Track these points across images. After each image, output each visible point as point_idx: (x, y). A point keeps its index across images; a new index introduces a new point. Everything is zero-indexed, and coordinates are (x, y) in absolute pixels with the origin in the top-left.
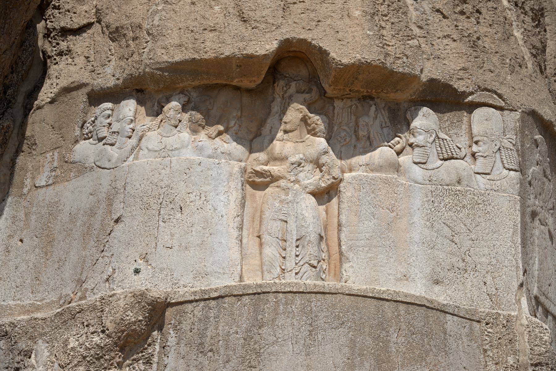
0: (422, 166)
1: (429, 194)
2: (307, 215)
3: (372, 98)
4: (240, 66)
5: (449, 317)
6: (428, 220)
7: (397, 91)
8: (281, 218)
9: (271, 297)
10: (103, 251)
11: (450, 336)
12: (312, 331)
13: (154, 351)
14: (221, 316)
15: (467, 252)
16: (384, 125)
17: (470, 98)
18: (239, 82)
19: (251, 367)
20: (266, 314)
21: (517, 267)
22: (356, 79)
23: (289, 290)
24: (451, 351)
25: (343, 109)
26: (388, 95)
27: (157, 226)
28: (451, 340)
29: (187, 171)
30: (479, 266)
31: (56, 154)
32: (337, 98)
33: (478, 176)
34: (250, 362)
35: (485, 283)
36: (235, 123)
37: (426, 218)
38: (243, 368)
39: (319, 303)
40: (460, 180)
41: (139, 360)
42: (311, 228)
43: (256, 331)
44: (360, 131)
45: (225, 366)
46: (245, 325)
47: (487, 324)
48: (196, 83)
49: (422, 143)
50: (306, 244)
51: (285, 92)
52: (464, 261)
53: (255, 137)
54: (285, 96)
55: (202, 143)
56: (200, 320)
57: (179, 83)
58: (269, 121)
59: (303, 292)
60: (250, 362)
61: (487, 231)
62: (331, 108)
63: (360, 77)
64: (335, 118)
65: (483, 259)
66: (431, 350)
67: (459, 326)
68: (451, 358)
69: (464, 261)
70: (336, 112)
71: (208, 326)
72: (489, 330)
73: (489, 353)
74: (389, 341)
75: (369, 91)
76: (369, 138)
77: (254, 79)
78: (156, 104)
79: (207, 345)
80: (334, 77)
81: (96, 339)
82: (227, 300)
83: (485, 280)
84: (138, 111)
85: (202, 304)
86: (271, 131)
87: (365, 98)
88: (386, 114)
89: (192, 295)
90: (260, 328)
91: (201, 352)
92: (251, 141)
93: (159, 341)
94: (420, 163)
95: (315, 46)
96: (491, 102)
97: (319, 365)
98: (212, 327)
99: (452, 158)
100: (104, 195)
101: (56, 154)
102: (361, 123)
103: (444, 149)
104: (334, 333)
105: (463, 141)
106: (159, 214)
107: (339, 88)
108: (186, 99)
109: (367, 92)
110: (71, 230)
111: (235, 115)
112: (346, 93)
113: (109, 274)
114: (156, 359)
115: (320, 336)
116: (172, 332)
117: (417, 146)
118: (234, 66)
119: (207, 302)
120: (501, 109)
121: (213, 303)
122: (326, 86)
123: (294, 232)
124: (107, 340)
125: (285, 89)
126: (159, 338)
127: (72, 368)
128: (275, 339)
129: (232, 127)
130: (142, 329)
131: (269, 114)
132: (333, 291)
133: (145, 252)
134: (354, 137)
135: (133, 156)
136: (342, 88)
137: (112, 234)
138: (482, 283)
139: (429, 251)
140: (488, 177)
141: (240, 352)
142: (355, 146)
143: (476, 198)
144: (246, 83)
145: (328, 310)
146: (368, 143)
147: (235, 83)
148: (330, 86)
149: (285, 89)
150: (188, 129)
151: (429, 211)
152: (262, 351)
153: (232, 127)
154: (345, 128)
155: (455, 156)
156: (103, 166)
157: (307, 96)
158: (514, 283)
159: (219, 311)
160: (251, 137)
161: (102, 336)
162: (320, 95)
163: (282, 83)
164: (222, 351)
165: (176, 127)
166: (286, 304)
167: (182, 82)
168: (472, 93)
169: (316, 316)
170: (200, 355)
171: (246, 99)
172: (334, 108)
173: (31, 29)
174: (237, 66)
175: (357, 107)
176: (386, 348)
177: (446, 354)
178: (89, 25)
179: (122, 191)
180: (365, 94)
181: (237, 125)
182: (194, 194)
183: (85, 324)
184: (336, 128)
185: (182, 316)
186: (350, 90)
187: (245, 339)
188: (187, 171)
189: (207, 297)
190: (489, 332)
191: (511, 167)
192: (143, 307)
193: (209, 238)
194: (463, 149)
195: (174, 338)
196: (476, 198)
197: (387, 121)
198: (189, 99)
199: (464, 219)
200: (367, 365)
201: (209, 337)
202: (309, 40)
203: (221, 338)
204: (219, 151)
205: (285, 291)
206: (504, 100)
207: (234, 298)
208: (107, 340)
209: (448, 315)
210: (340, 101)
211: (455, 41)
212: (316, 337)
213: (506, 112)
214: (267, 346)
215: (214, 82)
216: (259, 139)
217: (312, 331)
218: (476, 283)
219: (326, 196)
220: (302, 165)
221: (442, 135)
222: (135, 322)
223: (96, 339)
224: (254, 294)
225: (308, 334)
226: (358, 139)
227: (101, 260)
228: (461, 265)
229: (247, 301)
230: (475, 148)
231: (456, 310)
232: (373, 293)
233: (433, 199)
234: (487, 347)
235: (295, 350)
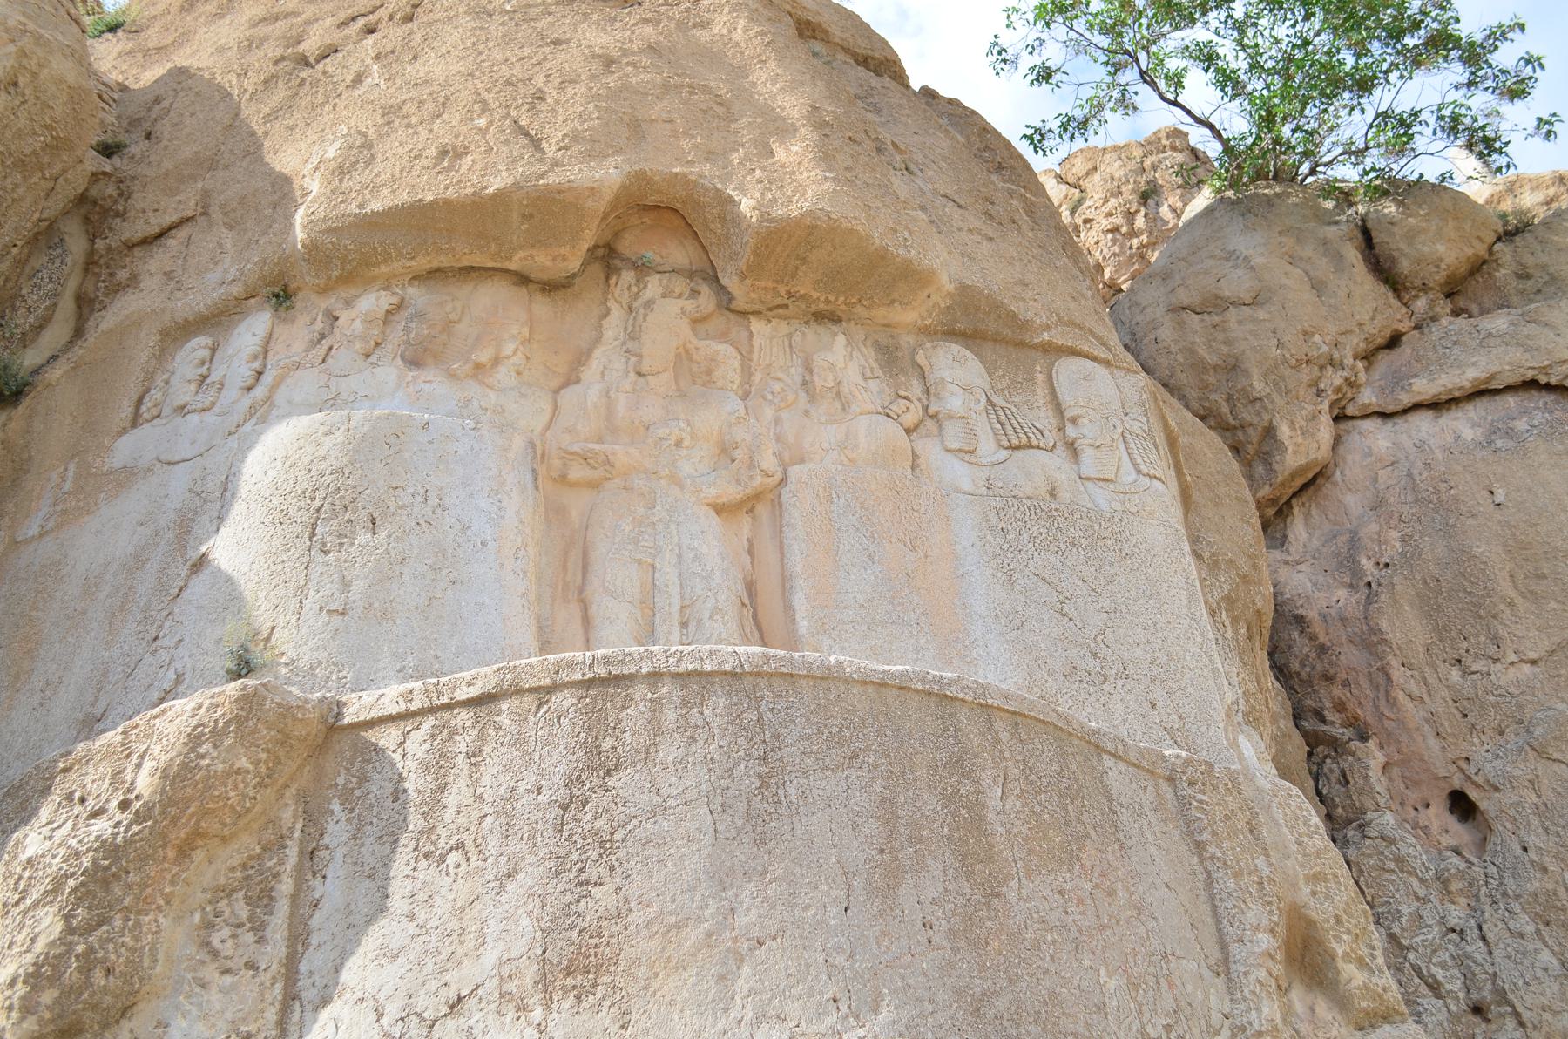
0: (967, 457)
1: (993, 516)
2: (705, 549)
3: (836, 319)
4: (531, 216)
5: (1108, 762)
6: (999, 568)
7: (893, 301)
8: (638, 556)
9: (639, 691)
10: (156, 639)
11: (1122, 805)
12: (769, 775)
13: (281, 863)
14: (487, 749)
15: (1100, 637)
16: (869, 374)
17: (1046, 336)
18: (526, 258)
19: (587, 883)
20: (627, 735)
21: (1215, 670)
22: (804, 260)
23: (691, 667)
24: (1130, 843)
25: (771, 339)
26: (873, 313)
27: (306, 560)
28: (1125, 817)
29: (393, 440)
30: (1131, 669)
31: (72, 467)
32: (757, 313)
33: (1089, 485)
34: (582, 870)
35: (1153, 706)
36: (516, 350)
37: (993, 564)
38: (560, 887)
39: (781, 704)
40: (1053, 489)
41: (234, 891)
42: (718, 579)
43: (597, 781)
44: (816, 378)
45: (502, 887)
46: (562, 768)
47: (1192, 784)
48: (423, 263)
49: (962, 413)
50: (707, 614)
51: (636, 296)
52: (1095, 656)
53: (567, 384)
54: (635, 305)
55: (434, 385)
56: (425, 767)
57: (378, 265)
58: (597, 353)
59: (733, 674)
60: (582, 870)
61: (1133, 593)
62: (745, 334)
63: (813, 257)
64: (755, 356)
65: (1138, 652)
66: (1088, 836)
67: (1134, 786)
68: (1134, 859)
69: (1095, 656)
70: (756, 342)
71: (450, 779)
72: (1200, 796)
73: (1212, 849)
74: (984, 806)
75: (832, 298)
76: (838, 395)
77: (563, 251)
78: (320, 317)
79: (444, 834)
80: (755, 253)
81: (102, 827)
82: (505, 706)
83: (1150, 697)
84: (275, 336)
85: (429, 722)
86: (603, 374)
87: (819, 317)
88: (870, 353)
89: (400, 700)
90: (608, 773)
91: (427, 855)
92: (557, 391)
93: (297, 834)
94: (960, 451)
95: (707, 189)
96: (1086, 348)
97: (798, 870)
98: (463, 781)
99: (1031, 447)
100: (172, 515)
101: (72, 467)
102: (818, 362)
103: (1009, 427)
104: (833, 782)
105: (1044, 418)
106: (313, 534)
107: (763, 284)
108: (395, 300)
109: (827, 301)
110: (84, 613)
111: (515, 332)
112: (778, 301)
113: (166, 686)
114: (286, 886)
115: (792, 790)
116: (336, 806)
117: (951, 417)
118: (515, 217)
119: (446, 715)
120: (1107, 363)
121: (464, 717)
122: (730, 281)
123: (675, 590)
124: (135, 828)
125: (635, 289)
126: (299, 826)
127: (26, 911)
128: (657, 800)
129: (508, 357)
130: (245, 796)
131: (598, 340)
132: (818, 673)
133: (269, 625)
134: (802, 394)
135: (254, 420)
136: (770, 285)
137: (185, 594)
138: (1147, 705)
139: (1014, 634)
140: (1112, 487)
141: (548, 843)
142: (807, 413)
143: (1097, 527)
144: (541, 262)
145: (808, 719)
146: (838, 405)
147: (513, 266)
148: (743, 277)
149: (635, 289)
150: (399, 361)
151: (998, 550)
152: (618, 836)
153: (508, 357)
154: (780, 375)
155: (1035, 442)
156: (177, 458)
157: (689, 305)
158: (1214, 704)
159: (482, 736)
160: (555, 383)
161: (118, 816)
162: (719, 306)
163: (628, 276)
164: (493, 845)
165: (368, 356)
166: (685, 704)
167: (385, 261)
168: (1047, 328)
169: (776, 736)
170: (424, 863)
171: (542, 307)
172: (751, 335)
173: (59, 251)
174: (524, 216)
175: (804, 334)
176: (977, 822)
177: (1121, 848)
178: (185, 221)
179: (218, 494)
180: (822, 306)
181: (519, 354)
182: (410, 490)
183: (77, 795)
184: (757, 377)
185: (369, 761)
186: (790, 295)
187: (565, 808)
188: (393, 440)
189: (445, 700)
190: (1201, 802)
191: (1152, 472)
192: (253, 732)
193: (449, 592)
194: (1046, 433)
195: (343, 824)
196: (1097, 527)
197: (875, 366)
198: (402, 301)
199: (1079, 567)
200: (935, 868)
201: (452, 809)
202: (693, 177)
203: (487, 809)
204: (475, 403)
205: (680, 670)
206: (1110, 350)
207: (527, 698)
208: (135, 828)
209: (1105, 757)
210: (763, 322)
211: (991, 239)
212: (781, 792)
213: (1118, 373)
214: (635, 822)
215: (466, 263)
216: (574, 390)
217: (769, 775)
218: (1133, 705)
219: (748, 518)
220: (686, 443)
221: (995, 399)
222: (228, 774)
223: (102, 827)
224: (589, 684)
225: (758, 784)
226: (812, 397)
227: (148, 658)
228: (1092, 664)
229: (566, 704)
230: (1071, 432)
231: (1120, 746)
232: (924, 682)
233: (1002, 524)
234: (1206, 836)
235: (721, 828)
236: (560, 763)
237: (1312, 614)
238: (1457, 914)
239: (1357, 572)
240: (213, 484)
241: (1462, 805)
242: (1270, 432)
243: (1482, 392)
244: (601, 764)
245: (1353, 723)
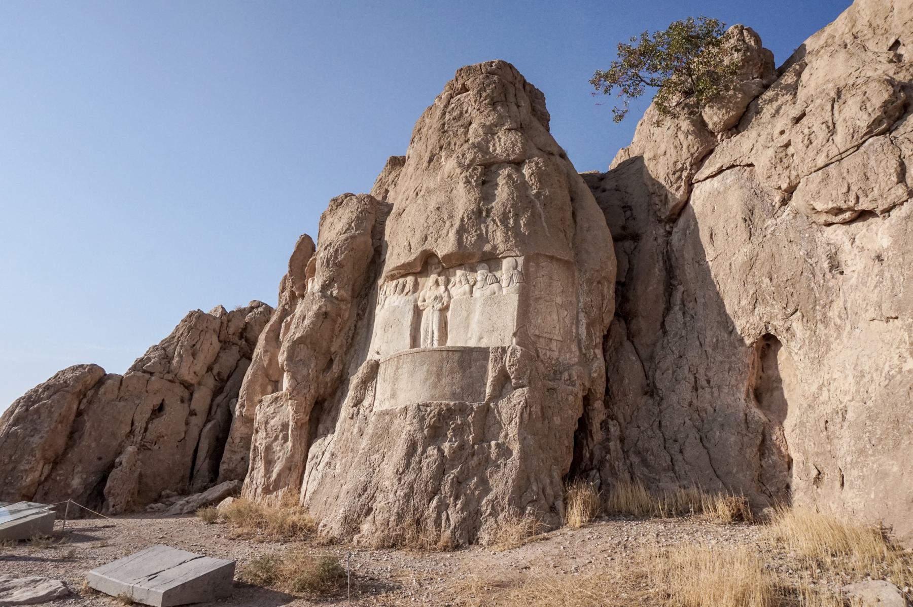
236: (394, 368)
243: (720, 171)
244: (397, 368)
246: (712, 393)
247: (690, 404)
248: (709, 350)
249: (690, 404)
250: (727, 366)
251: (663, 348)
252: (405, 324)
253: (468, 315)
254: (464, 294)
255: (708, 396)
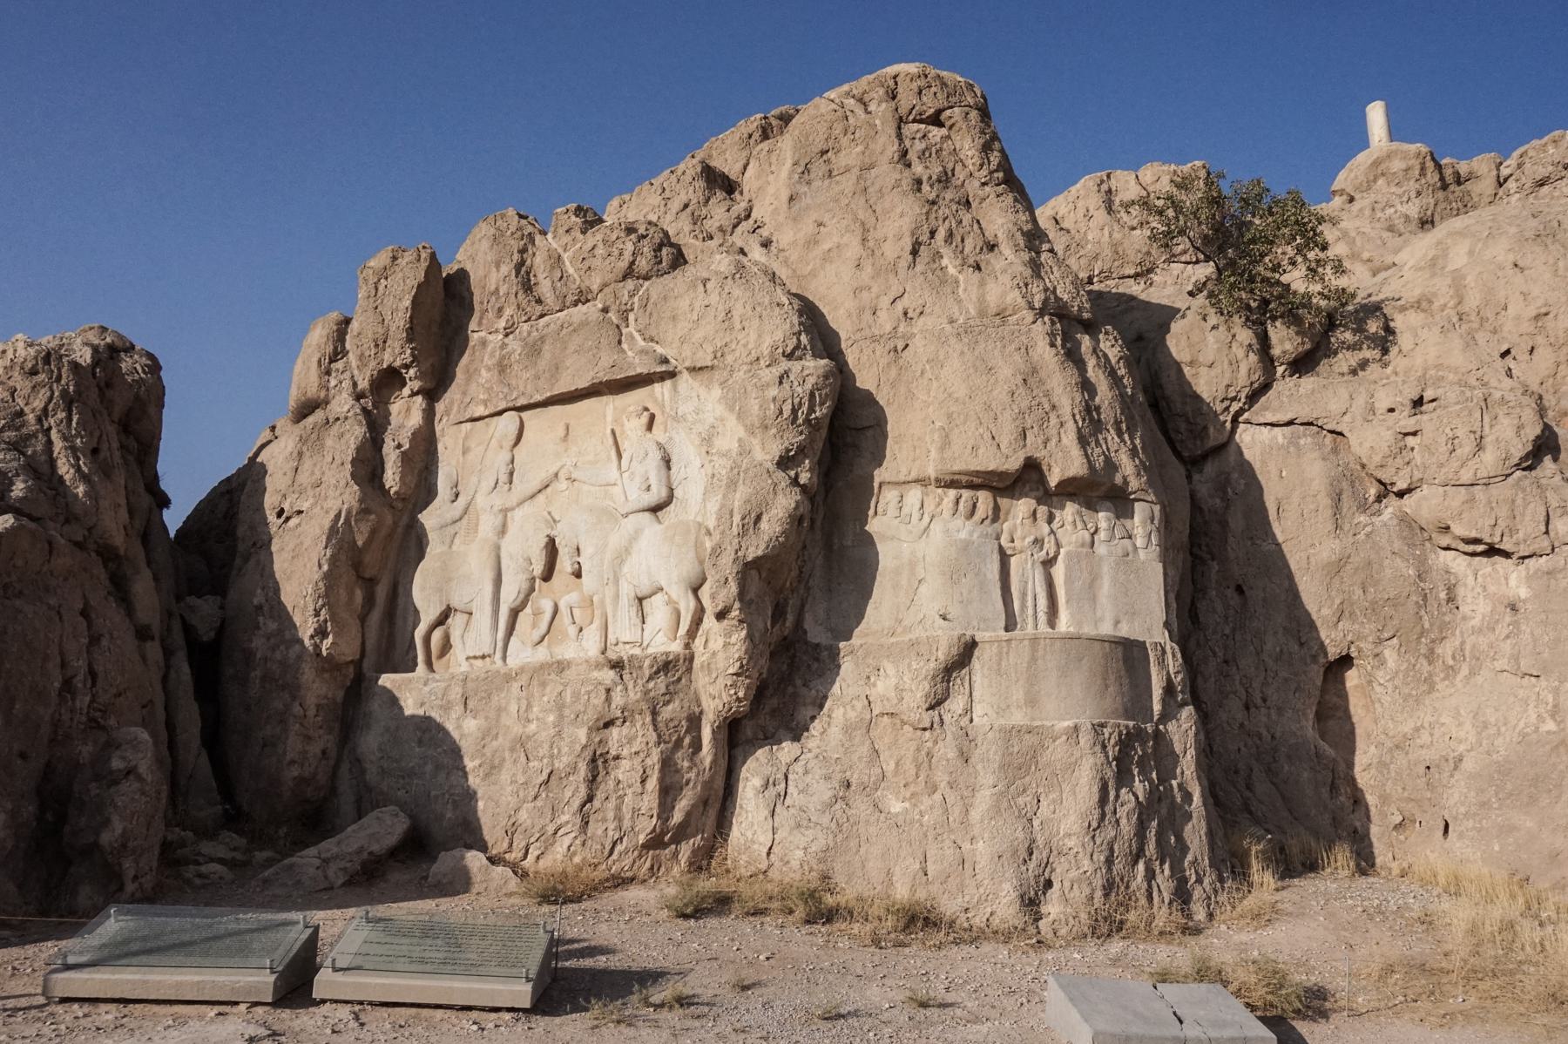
237: (1205, 508)
238: (1227, 631)
239: (1225, 493)
240: (920, 555)
241: (1239, 589)
242: (1205, 428)
244: (1034, 659)
245: (1210, 553)
246: (1269, 715)
247: (1242, 725)
248: (1270, 663)
249: (1242, 725)
250: (1293, 686)
251: (1198, 644)
252: (989, 576)
253: (1093, 581)
254: (1083, 545)
255: (1264, 719)
